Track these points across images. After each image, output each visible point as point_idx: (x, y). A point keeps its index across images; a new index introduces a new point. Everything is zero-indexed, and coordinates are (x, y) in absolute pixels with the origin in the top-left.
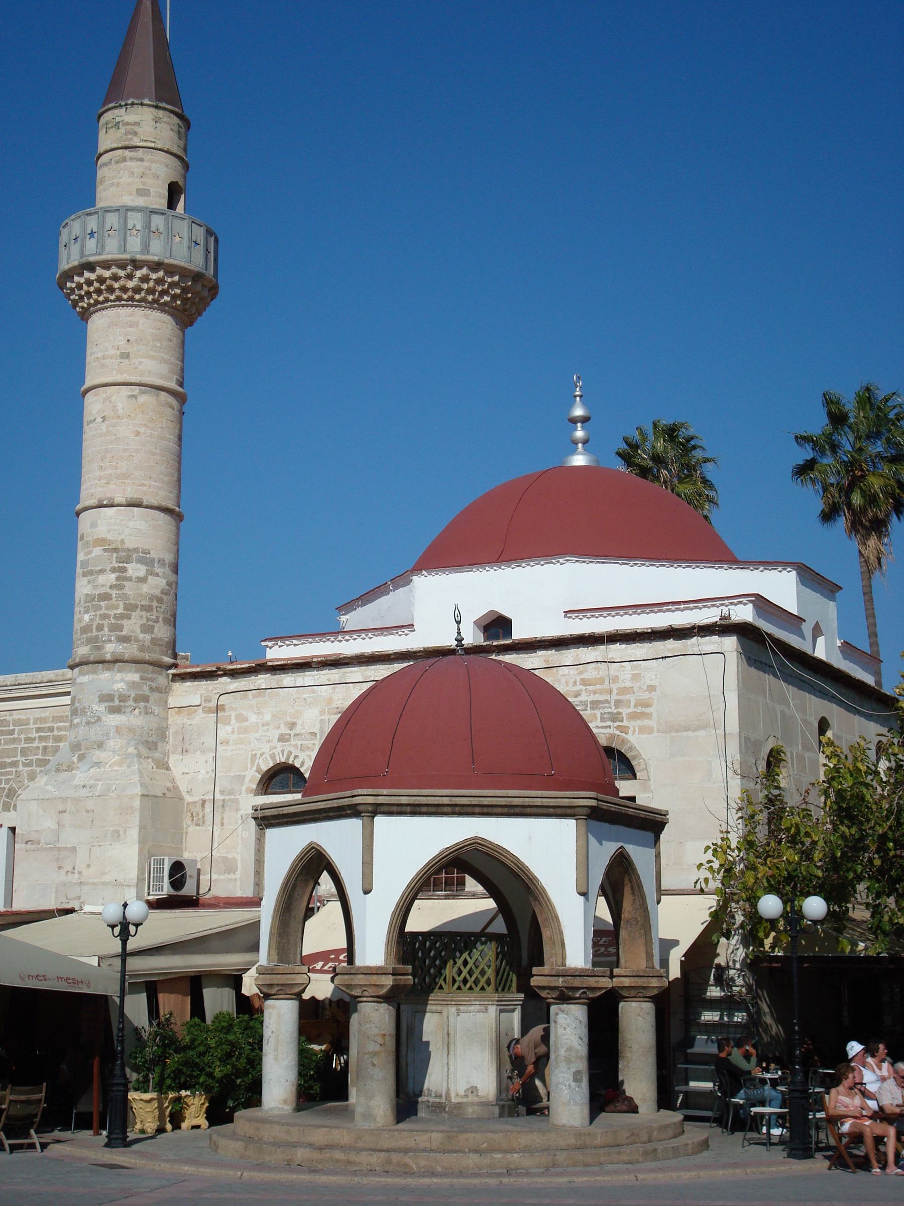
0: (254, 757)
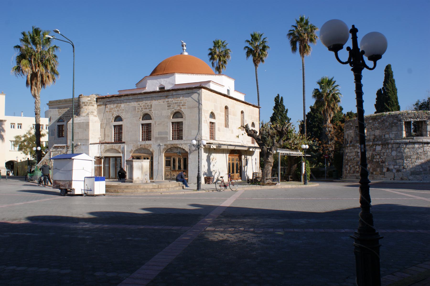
0: (113, 115)
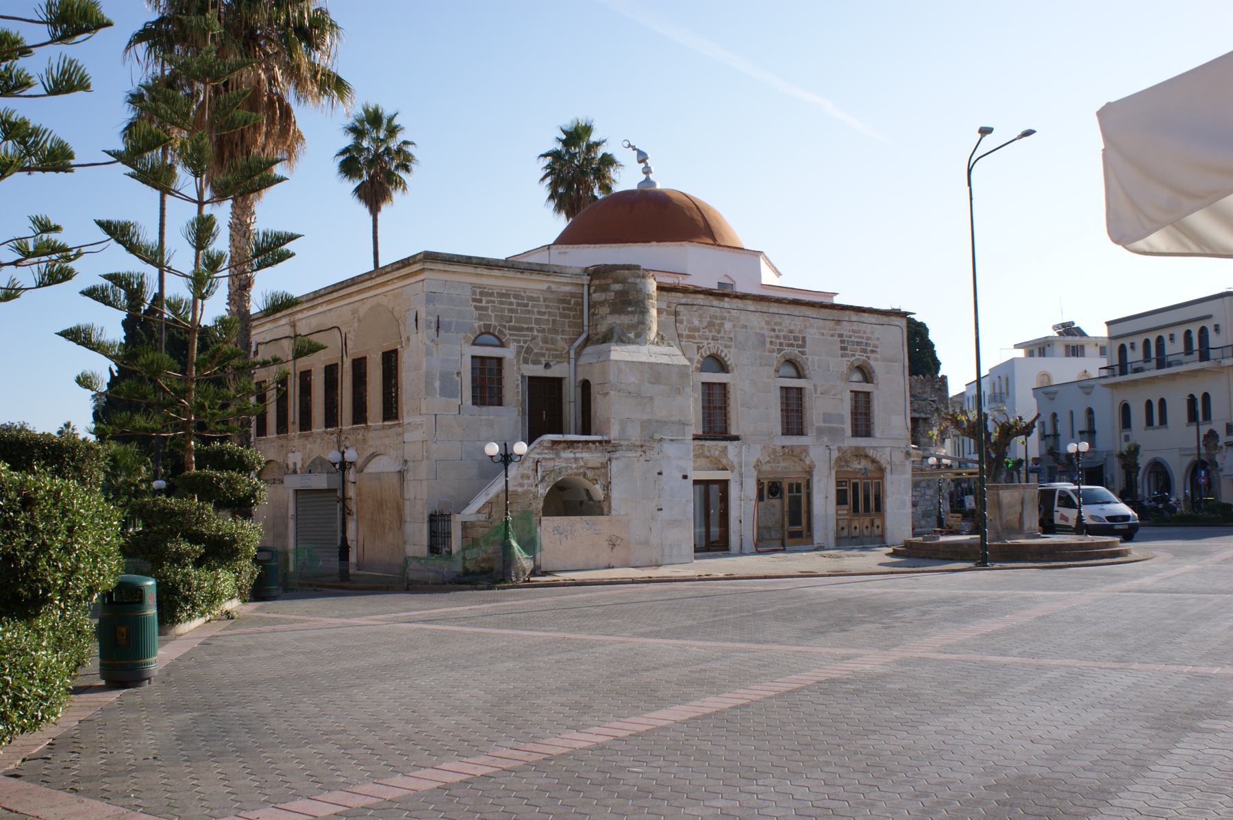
0: (699, 348)
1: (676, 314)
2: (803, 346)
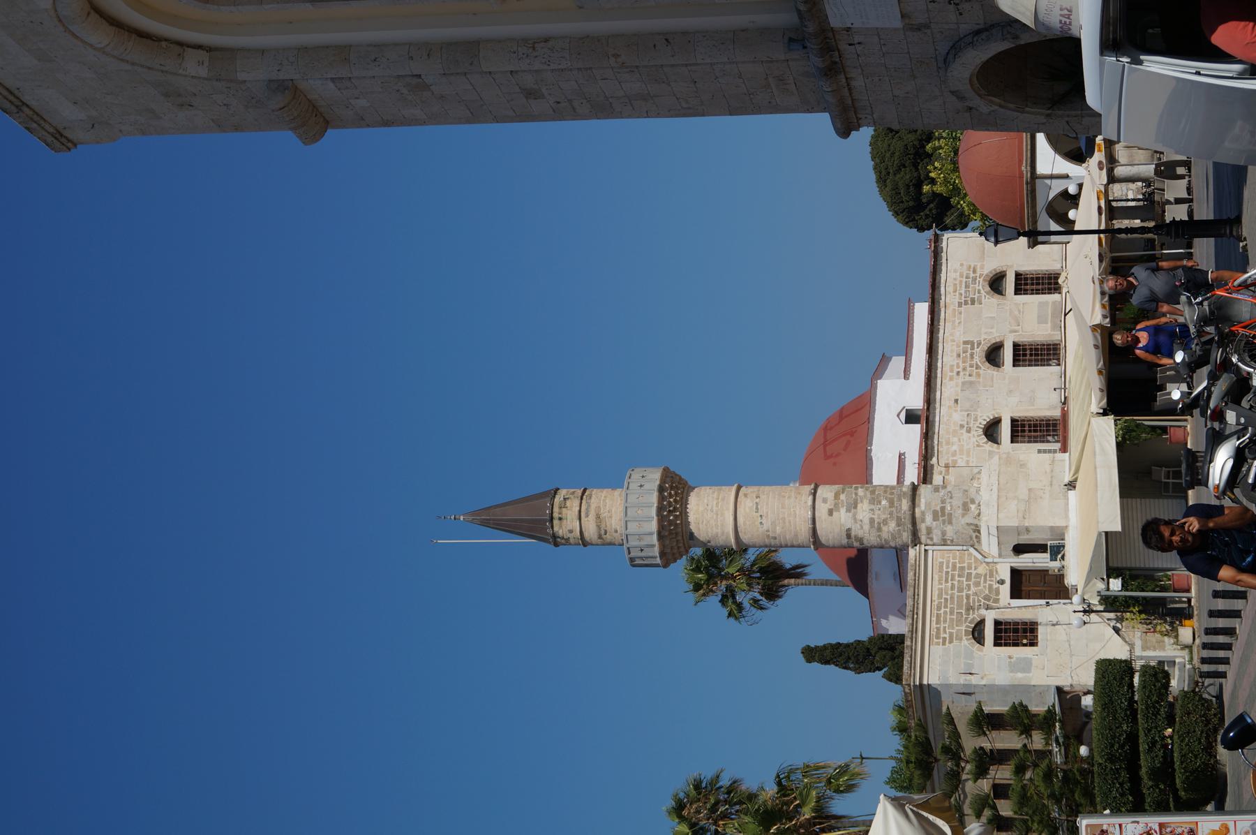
1: (947, 466)
2: (972, 343)
